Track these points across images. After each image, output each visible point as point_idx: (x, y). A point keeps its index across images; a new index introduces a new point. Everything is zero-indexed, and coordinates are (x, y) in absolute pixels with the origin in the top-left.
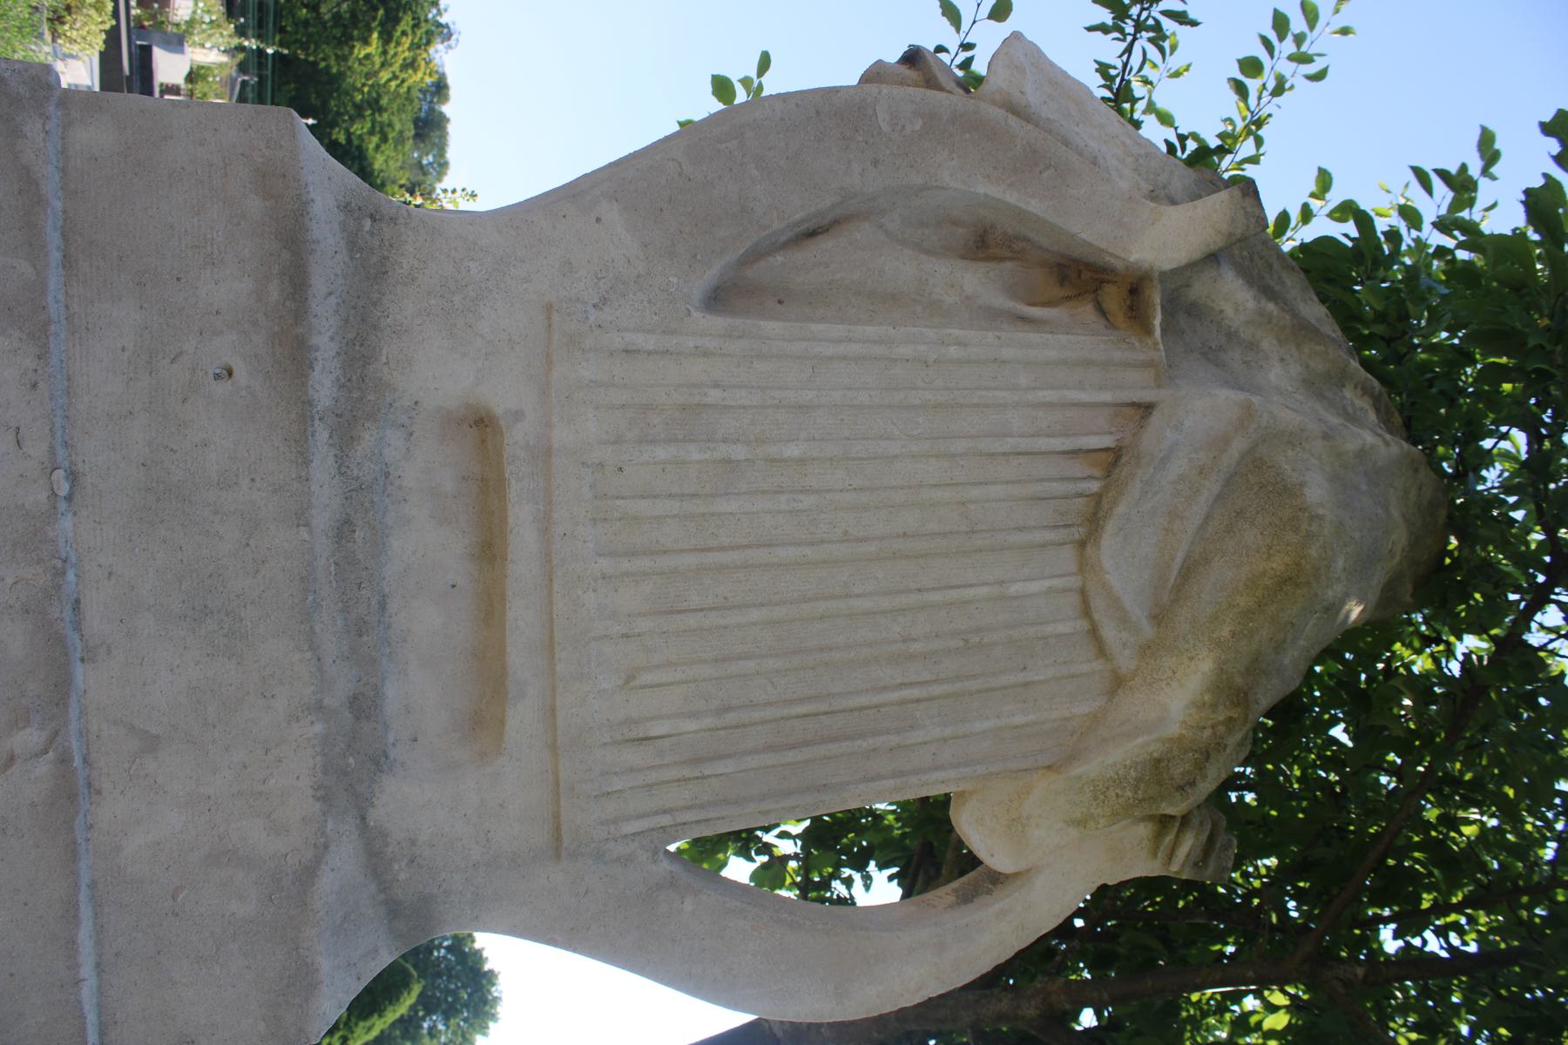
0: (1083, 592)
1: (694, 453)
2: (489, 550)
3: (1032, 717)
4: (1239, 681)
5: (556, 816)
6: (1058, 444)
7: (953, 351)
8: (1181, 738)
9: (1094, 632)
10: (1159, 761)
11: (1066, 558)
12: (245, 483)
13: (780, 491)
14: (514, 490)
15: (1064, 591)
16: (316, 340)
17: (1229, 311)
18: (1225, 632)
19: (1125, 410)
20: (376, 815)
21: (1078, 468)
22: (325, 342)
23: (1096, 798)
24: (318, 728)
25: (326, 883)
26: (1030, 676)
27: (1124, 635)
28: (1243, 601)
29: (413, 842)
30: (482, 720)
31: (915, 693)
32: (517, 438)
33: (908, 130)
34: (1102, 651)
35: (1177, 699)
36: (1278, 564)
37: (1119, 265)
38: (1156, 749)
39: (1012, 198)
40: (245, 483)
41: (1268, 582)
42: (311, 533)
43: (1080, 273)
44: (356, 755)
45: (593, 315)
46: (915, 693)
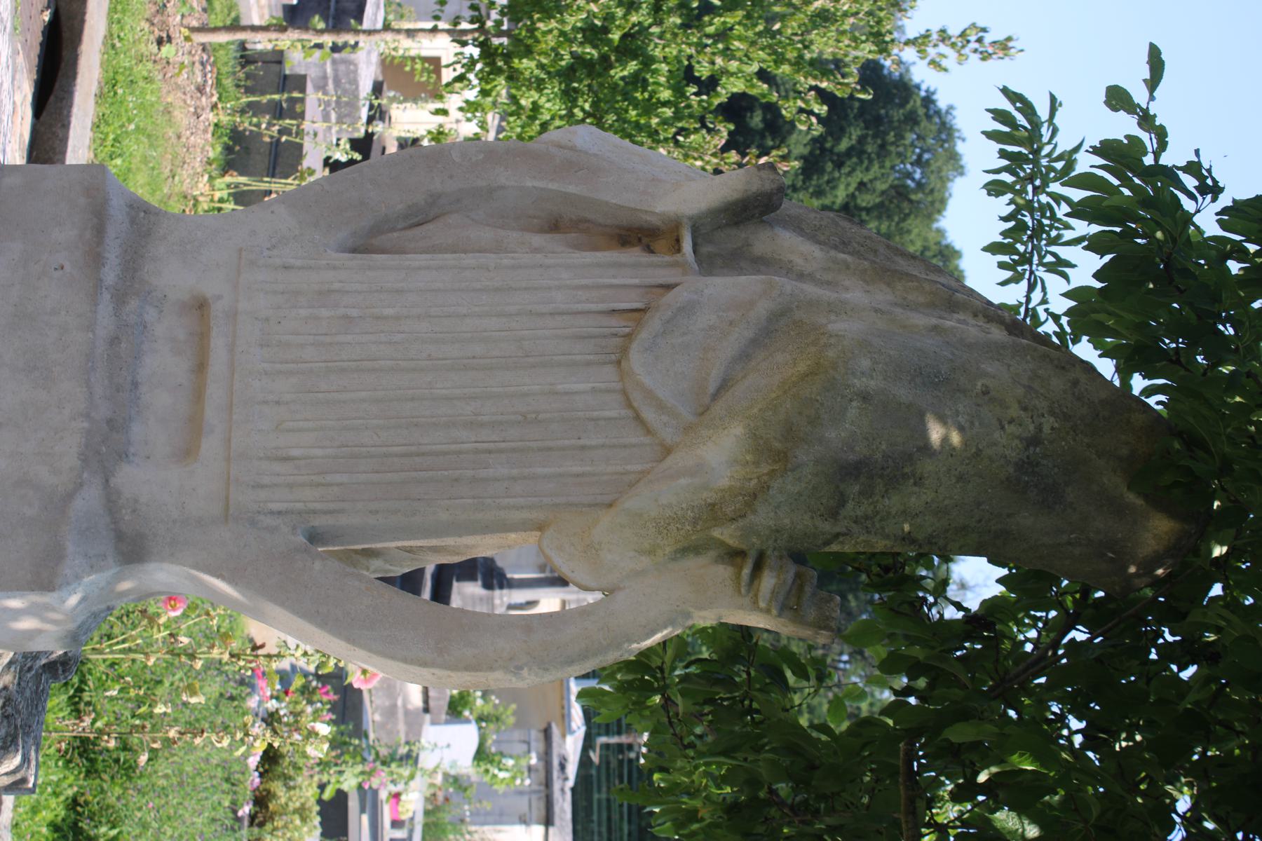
0: (624, 392)
1: (324, 313)
2: (200, 367)
3: (588, 469)
4: (777, 445)
5: (227, 498)
6: (593, 307)
7: (505, 261)
8: (730, 488)
9: (638, 418)
10: (713, 505)
11: (609, 372)
12: (63, 313)
13: (382, 332)
14: (214, 333)
15: (608, 391)
16: (107, 255)
17: (798, 261)
18: (755, 410)
19: (654, 290)
20: (113, 481)
21: (614, 321)
22: (113, 254)
23: (660, 533)
24: (86, 425)
25: (79, 504)
26: (582, 442)
27: (665, 418)
28: (773, 395)
29: (136, 501)
30: (187, 452)
31: (485, 445)
32: (217, 309)
33: (474, 159)
34: (648, 431)
35: (720, 456)
36: (802, 367)
37: (655, 221)
38: (709, 496)
39: (553, 186)
40: (63, 313)
41: (794, 379)
42: (94, 334)
43: (640, 240)
44: (108, 446)
45: (266, 253)
46: (485, 445)
